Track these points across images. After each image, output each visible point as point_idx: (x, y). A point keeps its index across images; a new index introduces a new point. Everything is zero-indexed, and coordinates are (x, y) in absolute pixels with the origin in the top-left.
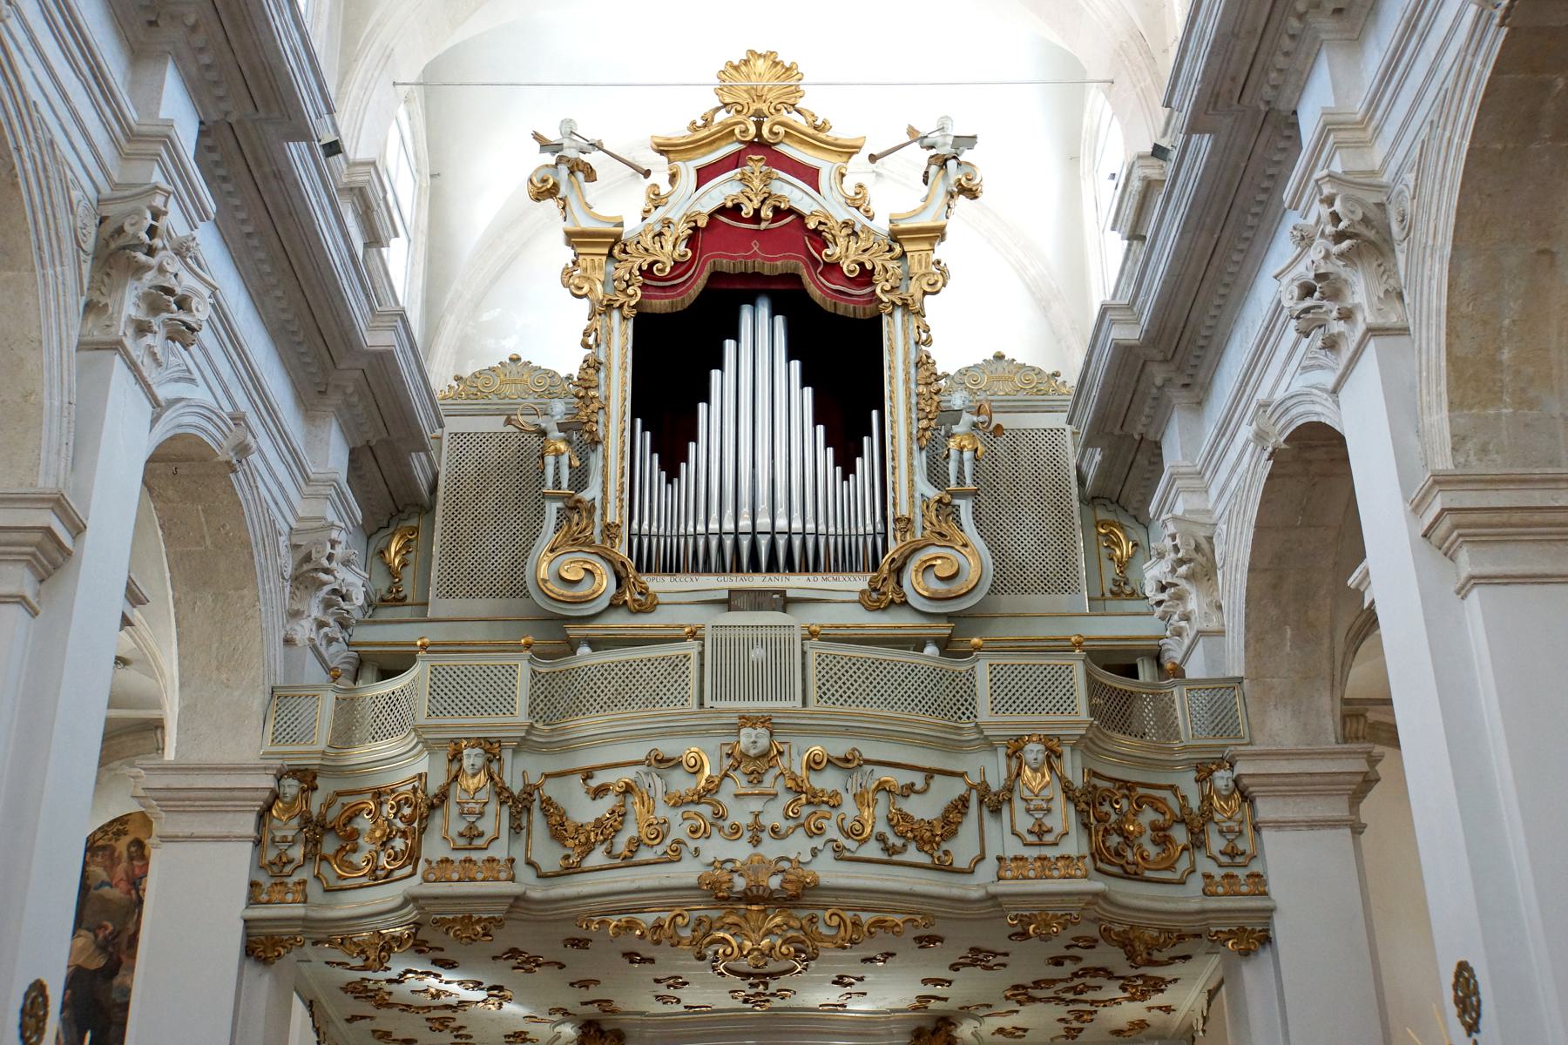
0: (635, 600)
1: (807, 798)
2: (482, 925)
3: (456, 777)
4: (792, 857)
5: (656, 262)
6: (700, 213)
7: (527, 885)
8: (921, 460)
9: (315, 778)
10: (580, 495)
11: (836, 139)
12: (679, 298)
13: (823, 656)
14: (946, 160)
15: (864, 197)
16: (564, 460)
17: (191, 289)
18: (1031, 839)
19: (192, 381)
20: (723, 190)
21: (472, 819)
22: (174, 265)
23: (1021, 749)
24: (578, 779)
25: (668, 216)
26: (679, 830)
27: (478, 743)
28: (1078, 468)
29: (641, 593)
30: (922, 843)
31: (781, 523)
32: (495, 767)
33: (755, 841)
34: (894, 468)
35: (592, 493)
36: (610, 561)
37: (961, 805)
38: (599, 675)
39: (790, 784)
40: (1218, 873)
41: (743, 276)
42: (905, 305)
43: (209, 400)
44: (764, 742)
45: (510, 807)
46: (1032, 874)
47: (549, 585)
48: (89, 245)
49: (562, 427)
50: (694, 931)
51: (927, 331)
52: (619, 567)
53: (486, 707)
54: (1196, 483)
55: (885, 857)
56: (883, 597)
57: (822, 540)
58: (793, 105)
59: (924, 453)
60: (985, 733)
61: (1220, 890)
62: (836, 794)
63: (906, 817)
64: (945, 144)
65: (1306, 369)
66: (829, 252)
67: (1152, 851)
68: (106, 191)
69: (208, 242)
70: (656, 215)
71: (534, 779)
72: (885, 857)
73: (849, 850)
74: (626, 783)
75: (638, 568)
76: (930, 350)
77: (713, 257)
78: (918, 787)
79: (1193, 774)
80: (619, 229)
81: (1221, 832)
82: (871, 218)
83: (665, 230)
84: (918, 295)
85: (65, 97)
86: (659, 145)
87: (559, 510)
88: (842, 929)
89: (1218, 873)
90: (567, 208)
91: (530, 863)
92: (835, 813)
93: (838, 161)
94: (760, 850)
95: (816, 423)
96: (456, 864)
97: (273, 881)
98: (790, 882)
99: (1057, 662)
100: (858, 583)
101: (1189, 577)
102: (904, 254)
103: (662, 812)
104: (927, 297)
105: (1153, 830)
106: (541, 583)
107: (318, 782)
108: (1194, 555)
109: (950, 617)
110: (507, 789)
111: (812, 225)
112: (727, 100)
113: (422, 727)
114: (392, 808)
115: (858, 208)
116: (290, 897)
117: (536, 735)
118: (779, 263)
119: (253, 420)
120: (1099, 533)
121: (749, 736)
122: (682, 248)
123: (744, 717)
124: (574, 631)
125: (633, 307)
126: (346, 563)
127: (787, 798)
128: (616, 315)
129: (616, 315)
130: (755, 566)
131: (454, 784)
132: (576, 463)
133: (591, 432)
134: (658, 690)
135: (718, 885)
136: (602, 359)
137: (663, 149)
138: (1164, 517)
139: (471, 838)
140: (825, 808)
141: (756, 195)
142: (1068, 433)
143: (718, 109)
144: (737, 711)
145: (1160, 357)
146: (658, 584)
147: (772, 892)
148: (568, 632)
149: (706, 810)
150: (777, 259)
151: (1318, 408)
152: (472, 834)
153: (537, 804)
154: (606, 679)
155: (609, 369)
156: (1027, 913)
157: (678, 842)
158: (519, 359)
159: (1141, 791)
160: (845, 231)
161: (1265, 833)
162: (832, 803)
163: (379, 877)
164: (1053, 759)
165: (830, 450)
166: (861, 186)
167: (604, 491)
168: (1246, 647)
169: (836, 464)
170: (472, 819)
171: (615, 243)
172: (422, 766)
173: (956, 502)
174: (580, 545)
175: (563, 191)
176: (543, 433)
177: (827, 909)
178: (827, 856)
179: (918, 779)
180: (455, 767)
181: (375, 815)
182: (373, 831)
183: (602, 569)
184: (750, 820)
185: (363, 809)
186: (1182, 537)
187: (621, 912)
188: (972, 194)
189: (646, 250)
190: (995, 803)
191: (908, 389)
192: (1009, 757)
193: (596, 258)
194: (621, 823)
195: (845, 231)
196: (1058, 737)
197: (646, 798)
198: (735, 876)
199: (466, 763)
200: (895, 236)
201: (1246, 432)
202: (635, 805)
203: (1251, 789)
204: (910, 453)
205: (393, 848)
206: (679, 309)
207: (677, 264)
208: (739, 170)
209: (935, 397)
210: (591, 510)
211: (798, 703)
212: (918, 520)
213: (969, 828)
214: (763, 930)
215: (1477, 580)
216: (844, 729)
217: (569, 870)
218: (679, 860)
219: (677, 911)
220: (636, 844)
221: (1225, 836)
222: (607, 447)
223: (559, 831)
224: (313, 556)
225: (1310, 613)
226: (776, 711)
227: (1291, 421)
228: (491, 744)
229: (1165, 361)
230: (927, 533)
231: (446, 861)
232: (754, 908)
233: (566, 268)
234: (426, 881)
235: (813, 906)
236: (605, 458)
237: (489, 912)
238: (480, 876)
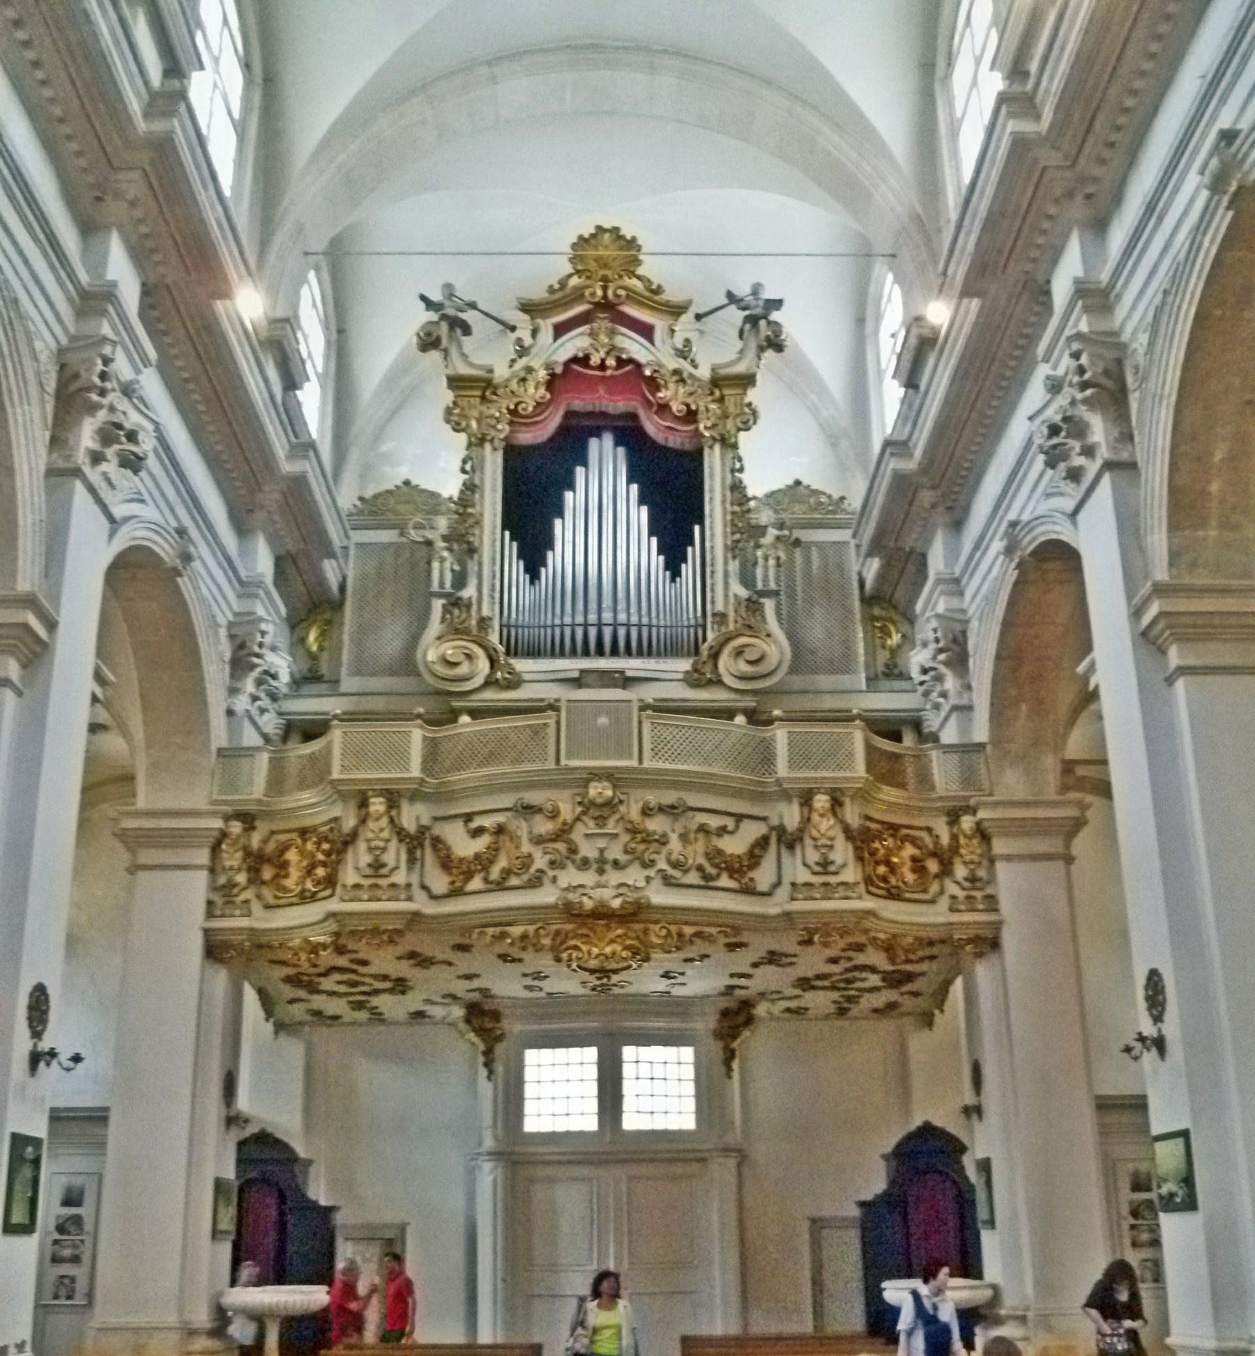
0: (505, 679)
4: (630, 882)
5: (520, 403)
6: (556, 362)
7: (421, 904)
8: (734, 566)
15: (690, 350)
16: (447, 565)
17: (136, 424)
18: (818, 869)
19: (142, 501)
20: (575, 343)
21: (377, 853)
22: (123, 404)
25: (532, 364)
26: (540, 862)
28: (860, 574)
31: (622, 617)
32: (394, 813)
33: (601, 871)
34: (713, 572)
35: (469, 592)
36: (485, 648)
37: (763, 843)
39: (629, 826)
41: (591, 414)
43: (157, 517)
44: (609, 793)
46: (818, 896)
48: (51, 386)
49: (445, 538)
50: (553, 939)
51: (740, 460)
52: (493, 653)
55: (702, 883)
60: (785, 786)
62: (664, 835)
63: (720, 852)
64: (757, 306)
65: (1049, 495)
68: (64, 341)
69: (152, 385)
71: (425, 821)
72: (702, 883)
75: (508, 653)
78: (730, 828)
84: (733, 431)
85: (26, 261)
86: (522, 304)
87: (444, 606)
91: (424, 887)
95: (651, 534)
100: (684, 665)
101: (947, 663)
102: (721, 400)
103: (526, 848)
109: (754, 692)
111: (648, 372)
112: (580, 267)
119: (194, 533)
120: (874, 627)
121: (596, 788)
122: (542, 391)
124: (457, 704)
126: (274, 649)
127: (625, 838)
128: (488, 447)
130: (600, 652)
132: (457, 568)
133: (469, 543)
136: (477, 482)
138: (928, 614)
140: (656, 845)
142: (852, 546)
143: (570, 276)
144: (585, 768)
146: (523, 665)
149: (561, 846)
151: (1057, 528)
152: (377, 866)
153: (427, 843)
159: (904, 831)
160: (675, 378)
172: (337, 811)
173: (762, 600)
175: (445, 342)
176: (429, 543)
178: (657, 883)
179: (730, 823)
180: (363, 811)
187: (495, 925)
188: (778, 347)
189: (513, 392)
190: (790, 841)
191: (724, 509)
192: (802, 805)
193: (472, 400)
194: (495, 856)
195: (675, 378)
198: (585, 899)
199: (372, 809)
201: (998, 545)
204: (726, 562)
207: (538, 404)
210: (468, 606)
212: (732, 615)
215: (1183, 671)
217: (456, 892)
219: (539, 924)
220: (507, 873)
223: (447, 863)
227: (1034, 539)
229: (934, 488)
230: (739, 625)
231: (357, 886)
236: (480, 564)
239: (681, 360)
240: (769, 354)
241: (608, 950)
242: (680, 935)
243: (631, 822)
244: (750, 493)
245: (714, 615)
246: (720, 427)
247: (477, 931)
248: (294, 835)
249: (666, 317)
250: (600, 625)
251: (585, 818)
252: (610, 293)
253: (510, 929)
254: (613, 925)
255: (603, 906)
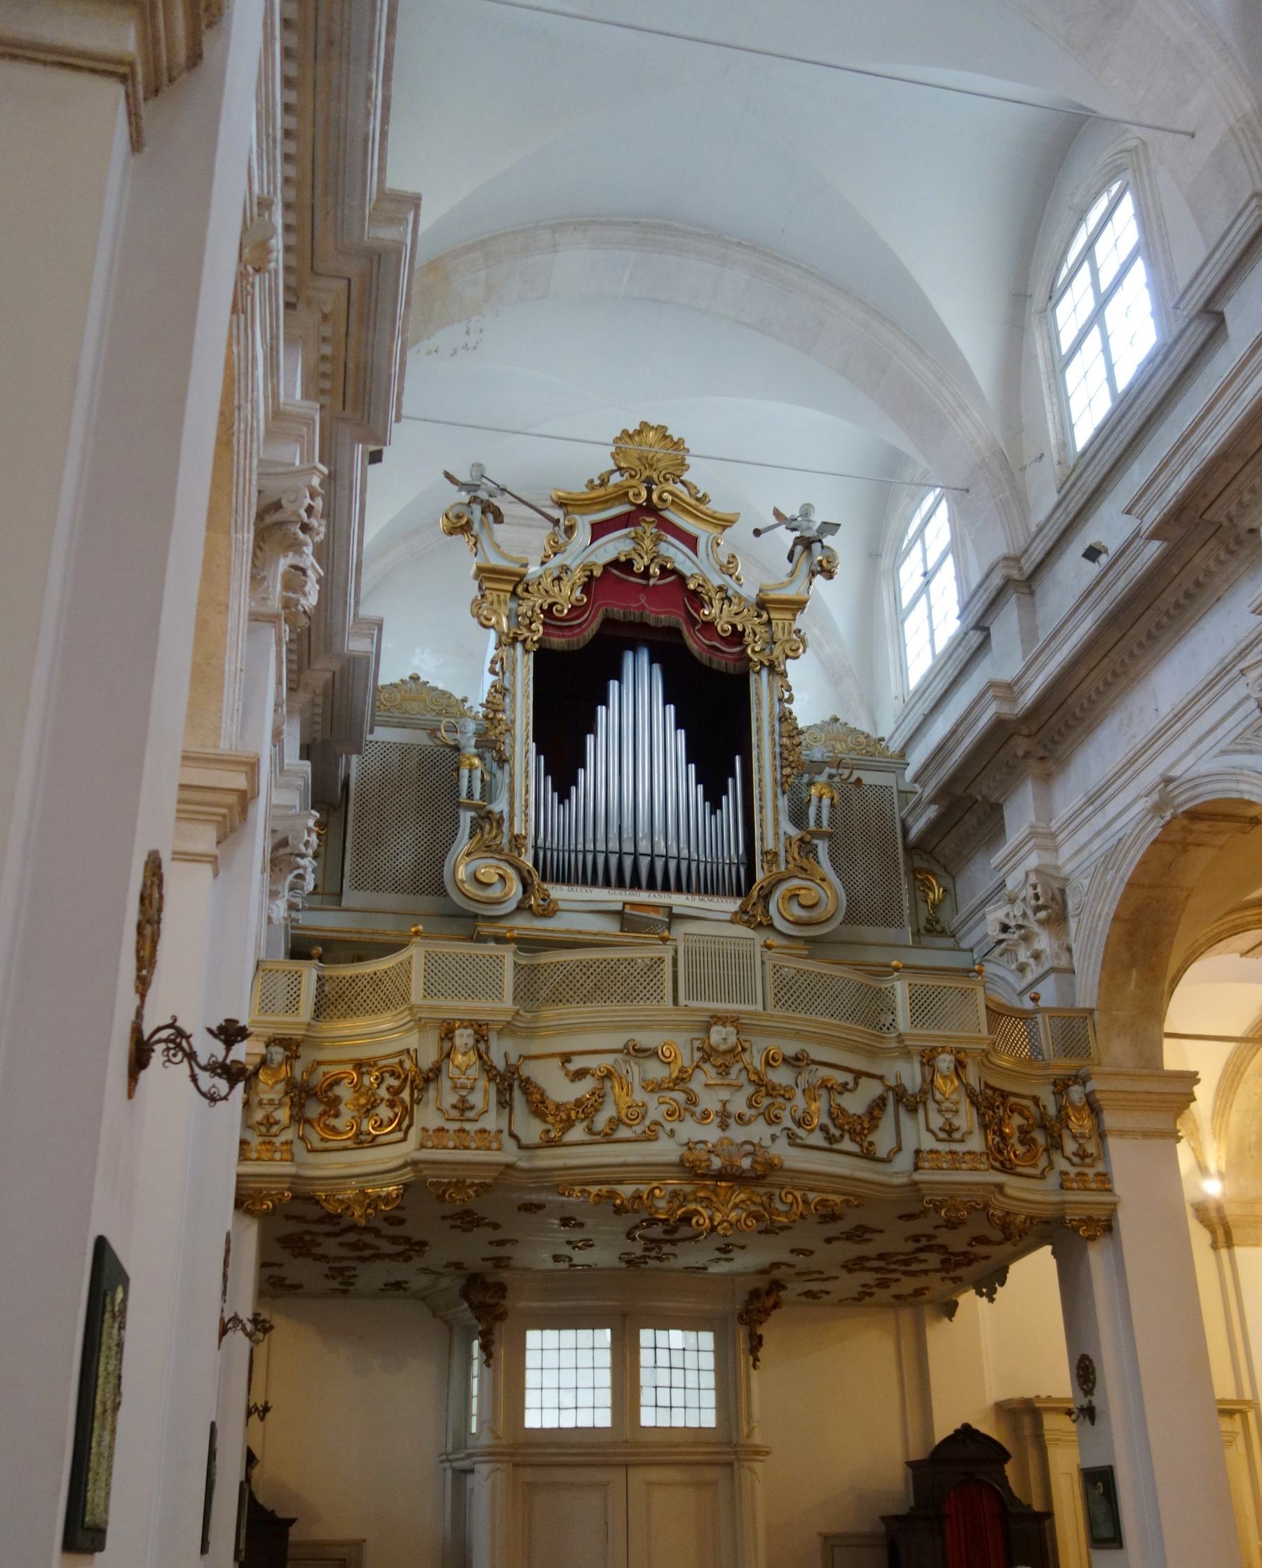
0: (539, 905)
1: (767, 1091)
2: (474, 1189)
3: (448, 1055)
4: (756, 1141)
6: (595, 564)
7: (510, 1154)
8: (783, 802)
9: (298, 1047)
10: (489, 807)
11: (715, 512)
12: (575, 639)
13: (777, 967)
14: (813, 542)
16: (478, 774)
18: (942, 1135)
20: (614, 546)
21: (464, 1093)
23: (934, 1058)
24: (557, 1062)
25: (567, 563)
26: (656, 1111)
27: (471, 1024)
29: (544, 900)
30: (856, 1135)
32: (482, 1046)
34: (761, 808)
36: (518, 869)
37: (880, 1103)
38: (577, 970)
39: (754, 1077)
40: (1073, 1171)
41: (631, 625)
42: (772, 668)
44: (732, 1040)
45: (497, 1084)
46: (945, 1165)
47: (466, 885)
50: (669, 1202)
51: (789, 689)
53: (477, 993)
54: (1048, 842)
55: (826, 1145)
56: (753, 919)
57: (694, 865)
58: (679, 477)
59: (786, 796)
60: (907, 1043)
61: (1075, 1185)
62: (789, 1089)
63: (843, 1111)
66: (706, 612)
67: (1020, 1150)
70: (555, 562)
71: (513, 1060)
72: (825, 1144)
73: (802, 1139)
74: (608, 1070)
75: (544, 879)
76: (790, 706)
77: (604, 604)
78: (851, 1086)
79: (1051, 1088)
80: (522, 570)
81: (1074, 1137)
82: (741, 585)
83: (563, 575)
87: (473, 819)
88: (795, 1206)
89: (1073, 1171)
90: (478, 545)
91: (512, 1135)
92: (788, 1105)
93: (714, 532)
94: (728, 1134)
95: (689, 761)
96: (451, 1133)
97: (261, 1139)
98: (759, 1163)
99: (957, 985)
100: (733, 905)
101: (1041, 923)
102: (769, 622)
103: (639, 1096)
104: (789, 661)
105: (1020, 1133)
106: (459, 884)
107: (301, 1051)
108: (1050, 903)
110: (495, 1068)
111: (691, 586)
113: (420, 1007)
114: (377, 1078)
115: (731, 576)
116: (278, 1156)
117: (520, 1021)
118: (663, 616)
121: (719, 1033)
122: (578, 593)
123: (715, 1016)
124: (485, 929)
125: (534, 642)
127: (749, 1090)
128: (519, 647)
129: (519, 647)
130: (651, 886)
131: (446, 1061)
133: (499, 751)
134: (635, 988)
135: (698, 1163)
136: (507, 685)
137: (561, 504)
139: (463, 1111)
140: (780, 1100)
141: (647, 553)
144: (708, 1010)
145: (1025, 731)
146: (559, 892)
147: (744, 1171)
148: (479, 929)
149: (680, 1097)
150: (661, 613)
152: (463, 1107)
153: (516, 1083)
154: (585, 974)
155: (514, 695)
156: (940, 1198)
157: (657, 1123)
158: (419, 678)
159: (1013, 1100)
160: (719, 595)
161: (1112, 1142)
162: (787, 1096)
163: (362, 1141)
164: (960, 1070)
165: (700, 787)
166: (734, 557)
167: (511, 804)
168: (1100, 984)
169: (705, 799)
170: (464, 1093)
171: (519, 583)
172: (412, 1041)
173: (815, 841)
174: (492, 852)
177: (783, 1188)
178: (783, 1141)
179: (848, 1078)
180: (447, 1045)
181: (357, 1087)
182: (357, 1099)
183: (510, 872)
184: (718, 1107)
185: (343, 1079)
186: (1042, 887)
188: (829, 575)
189: (547, 592)
190: (909, 1102)
191: (773, 740)
192: (922, 1064)
193: (502, 594)
194: (601, 1104)
195: (719, 595)
196: (964, 1050)
197: (624, 1082)
198: (712, 1155)
200: (762, 605)
202: (613, 1090)
203: (1101, 1103)
204: (775, 796)
205: (377, 1115)
206: (575, 648)
208: (632, 529)
209: (797, 749)
210: (500, 821)
211: (760, 1007)
213: (887, 1123)
214: (731, 1204)
216: (794, 1032)
217: (551, 1143)
218: (656, 1139)
219: (655, 1184)
220: (616, 1122)
221: (1077, 1141)
222: (513, 766)
224: (290, 841)
225: (1153, 960)
226: (740, 1012)
227: (1197, 797)
228: (480, 1026)
230: (791, 866)
231: (441, 1130)
232: (723, 1184)
233: (475, 600)
234: (423, 1146)
235: (771, 1185)
236: (512, 776)
237: (480, 1177)
238: (473, 1145)
239: (727, 577)
240: (819, 580)
241: (733, 1216)
242: (806, 1202)
243: (757, 1073)
244: (801, 724)
245: (765, 853)
246: (767, 651)
247: (578, 1188)
248: (349, 1068)
249: (711, 529)
250: (636, 855)
251: (706, 1066)
252: (655, 497)
253: (618, 1188)
254: (736, 1188)
255: (732, 1165)
